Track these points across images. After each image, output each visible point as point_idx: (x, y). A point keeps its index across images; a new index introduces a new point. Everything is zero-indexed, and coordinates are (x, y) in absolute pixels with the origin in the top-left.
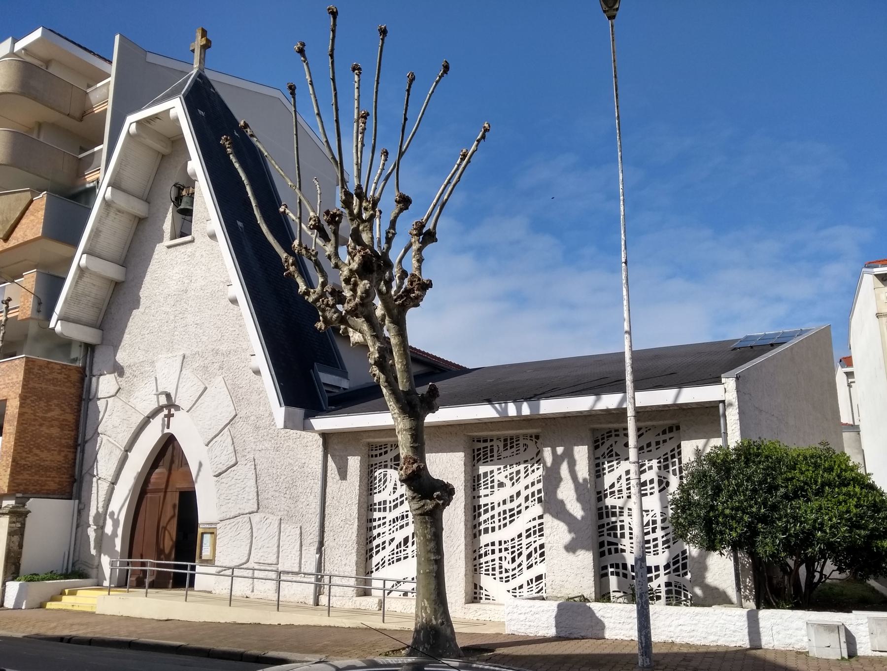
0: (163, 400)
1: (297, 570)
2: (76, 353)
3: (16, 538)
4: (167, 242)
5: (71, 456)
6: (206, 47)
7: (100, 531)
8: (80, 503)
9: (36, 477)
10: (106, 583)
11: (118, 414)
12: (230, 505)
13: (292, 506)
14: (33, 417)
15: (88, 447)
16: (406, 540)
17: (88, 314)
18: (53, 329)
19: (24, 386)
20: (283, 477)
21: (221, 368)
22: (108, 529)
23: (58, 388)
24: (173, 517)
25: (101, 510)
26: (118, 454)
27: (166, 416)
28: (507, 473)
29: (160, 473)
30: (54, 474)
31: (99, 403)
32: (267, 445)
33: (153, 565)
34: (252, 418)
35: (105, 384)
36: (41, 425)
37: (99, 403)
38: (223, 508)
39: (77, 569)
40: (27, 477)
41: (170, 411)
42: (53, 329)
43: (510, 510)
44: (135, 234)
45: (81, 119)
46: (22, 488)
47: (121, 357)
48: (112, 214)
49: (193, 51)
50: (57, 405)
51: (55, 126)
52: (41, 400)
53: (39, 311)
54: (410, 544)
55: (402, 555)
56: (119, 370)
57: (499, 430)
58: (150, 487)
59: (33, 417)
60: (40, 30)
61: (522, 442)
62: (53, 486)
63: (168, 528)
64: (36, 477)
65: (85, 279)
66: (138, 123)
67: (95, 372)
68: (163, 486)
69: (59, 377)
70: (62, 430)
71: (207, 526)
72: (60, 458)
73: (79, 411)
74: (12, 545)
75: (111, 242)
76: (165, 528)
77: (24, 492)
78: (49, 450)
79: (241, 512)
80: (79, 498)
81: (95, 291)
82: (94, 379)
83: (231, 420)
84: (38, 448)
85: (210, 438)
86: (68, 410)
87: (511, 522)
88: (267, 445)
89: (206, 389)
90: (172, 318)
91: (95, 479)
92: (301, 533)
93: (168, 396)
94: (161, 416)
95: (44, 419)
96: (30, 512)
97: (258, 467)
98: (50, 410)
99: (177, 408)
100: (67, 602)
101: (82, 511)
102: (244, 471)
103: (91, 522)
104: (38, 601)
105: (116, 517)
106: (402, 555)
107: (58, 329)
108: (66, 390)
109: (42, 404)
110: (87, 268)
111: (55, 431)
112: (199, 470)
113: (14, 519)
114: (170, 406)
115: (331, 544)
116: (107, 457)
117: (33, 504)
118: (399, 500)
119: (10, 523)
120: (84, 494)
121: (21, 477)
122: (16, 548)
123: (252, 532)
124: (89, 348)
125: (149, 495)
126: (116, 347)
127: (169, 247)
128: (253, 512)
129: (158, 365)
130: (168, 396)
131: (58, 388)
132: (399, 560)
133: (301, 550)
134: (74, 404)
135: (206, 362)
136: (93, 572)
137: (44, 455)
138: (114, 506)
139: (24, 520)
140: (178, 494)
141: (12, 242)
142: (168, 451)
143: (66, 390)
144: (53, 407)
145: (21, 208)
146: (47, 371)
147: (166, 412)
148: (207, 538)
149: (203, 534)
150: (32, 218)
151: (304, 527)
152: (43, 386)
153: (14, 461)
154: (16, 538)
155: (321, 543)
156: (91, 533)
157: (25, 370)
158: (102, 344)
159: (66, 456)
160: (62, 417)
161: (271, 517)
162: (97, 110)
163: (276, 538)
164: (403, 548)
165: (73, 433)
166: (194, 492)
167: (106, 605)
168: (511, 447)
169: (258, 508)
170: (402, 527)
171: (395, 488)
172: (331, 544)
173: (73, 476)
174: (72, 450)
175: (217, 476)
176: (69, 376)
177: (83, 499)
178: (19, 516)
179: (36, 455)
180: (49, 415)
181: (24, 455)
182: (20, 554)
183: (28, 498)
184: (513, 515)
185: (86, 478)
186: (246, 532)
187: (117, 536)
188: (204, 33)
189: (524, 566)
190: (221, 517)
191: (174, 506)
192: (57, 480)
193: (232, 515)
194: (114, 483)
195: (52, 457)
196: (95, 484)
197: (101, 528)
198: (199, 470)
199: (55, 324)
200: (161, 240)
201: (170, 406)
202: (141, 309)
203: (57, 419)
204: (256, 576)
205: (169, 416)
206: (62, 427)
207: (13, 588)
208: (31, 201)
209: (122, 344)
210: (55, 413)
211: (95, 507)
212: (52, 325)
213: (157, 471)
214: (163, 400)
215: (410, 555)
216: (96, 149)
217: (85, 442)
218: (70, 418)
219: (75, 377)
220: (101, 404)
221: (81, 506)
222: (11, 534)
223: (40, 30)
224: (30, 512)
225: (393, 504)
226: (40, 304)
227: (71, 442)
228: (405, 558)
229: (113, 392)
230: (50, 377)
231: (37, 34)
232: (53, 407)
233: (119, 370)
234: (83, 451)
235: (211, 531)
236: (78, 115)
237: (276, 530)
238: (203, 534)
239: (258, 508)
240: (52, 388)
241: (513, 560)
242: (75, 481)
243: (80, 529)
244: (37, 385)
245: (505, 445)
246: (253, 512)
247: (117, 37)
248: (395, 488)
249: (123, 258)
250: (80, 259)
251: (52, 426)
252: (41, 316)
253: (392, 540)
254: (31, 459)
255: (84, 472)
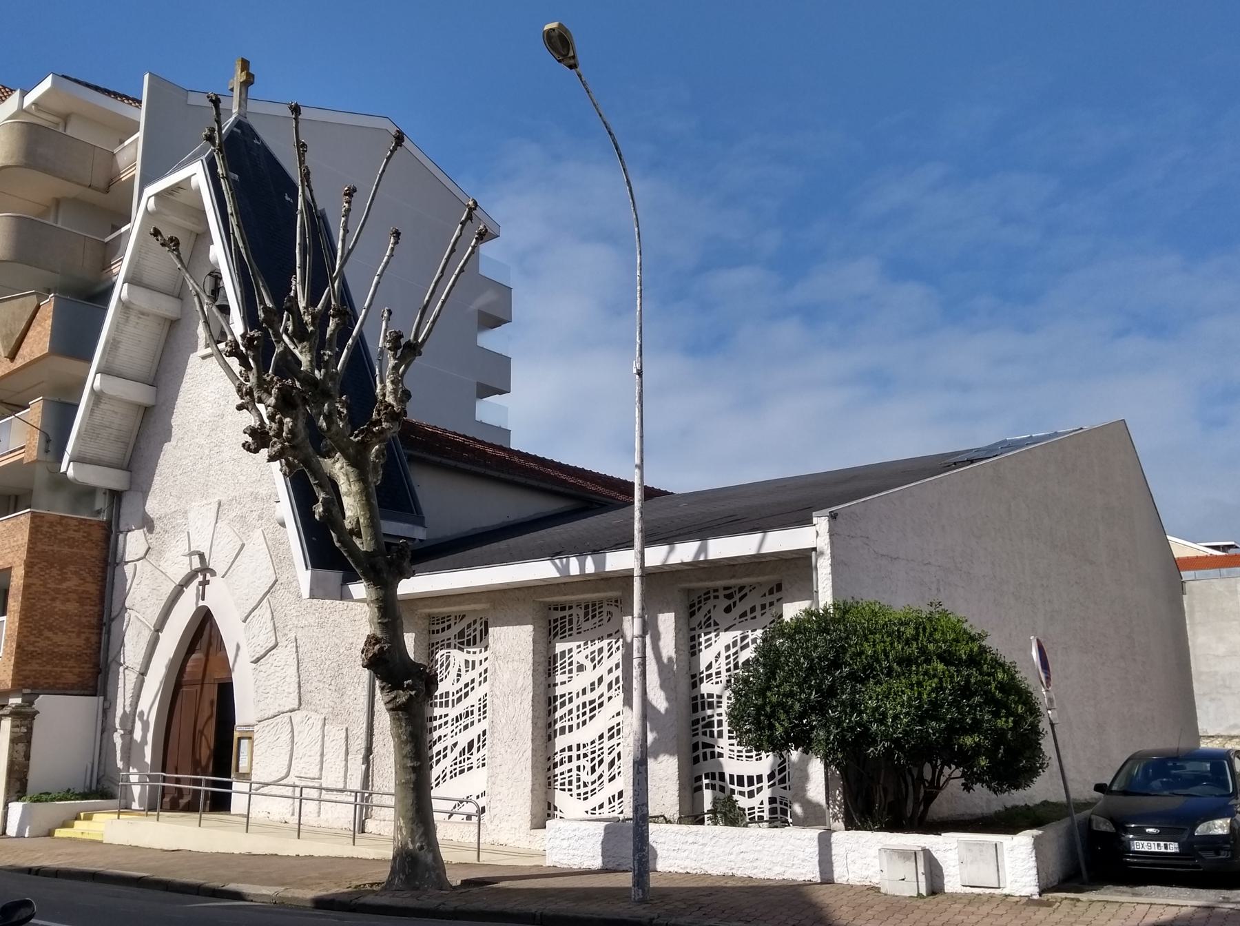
0: (196, 563)
1: (341, 786)
2: (101, 503)
3: (21, 747)
4: (202, 351)
5: (94, 639)
6: (248, 82)
7: (128, 737)
8: (105, 700)
9: (49, 668)
10: (135, 806)
11: (147, 582)
12: (268, 701)
13: (338, 701)
14: (42, 589)
15: (114, 625)
16: (471, 745)
17: (111, 451)
18: (65, 473)
19: (30, 550)
20: (328, 662)
21: (260, 518)
22: (137, 735)
23: (75, 550)
24: (211, 716)
25: (128, 709)
26: (147, 635)
27: (200, 584)
28: (588, 652)
29: (197, 660)
30: (72, 663)
31: (126, 567)
33: (209, 783)
35: (134, 543)
36: (53, 599)
37: (126, 567)
38: (261, 706)
39: (101, 788)
40: (36, 667)
42: (65, 473)
43: (592, 702)
44: (166, 341)
45: (107, 190)
46: (30, 681)
47: (152, 506)
48: (133, 319)
49: (232, 90)
50: (75, 573)
51: (77, 202)
52: (52, 566)
53: (47, 451)
54: (474, 750)
55: (466, 765)
56: (148, 524)
57: (573, 594)
58: (186, 678)
59: (42, 589)
60: (50, 78)
61: (605, 609)
62: (71, 678)
63: (205, 732)
64: (49, 668)
65: (102, 406)
66: (157, 195)
67: (122, 527)
68: (200, 677)
69: (77, 535)
70: (82, 605)
72: (80, 642)
73: (104, 579)
74: (16, 755)
75: (136, 353)
76: (202, 732)
77: (34, 686)
78: (64, 632)
79: (282, 709)
80: (105, 695)
81: (118, 421)
82: (121, 537)
83: (271, 587)
84: (50, 629)
85: (247, 611)
86: (90, 579)
87: (591, 718)
89: (243, 545)
90: (207, 452)
91: (121, 669)
92: (347, 737)
93: (202, 556)
94: (196, 583)
95: (57, 591)
96: (37, 712)
97: (300, 650)
98: (65, 579)
99: (213, 573)
100: (81, 829)
101: (107, 711)
102: (285, 654)
103: (117, 726)
104: (45, 826)
106: (466, 765)
107: (70, 473)
108: (85, 552)
109: (55, 572)
110: (101, 391)
111: (72, 607)
112: (237, 655)
113: (18, 723)
114: (202, 572)
115: (381, 751)
116: (135, 639)
117: (43, 703)
118: (464, 691)
119: (13, 727)
120: (110, 688)
121: (28, 668)
122: (21, 759)
123: (293, 736)
124: (116, 496)
125: (184, 689)
126: (145, 494)
127: (204, 358)
128: (293, 710)
129: (191, 515)
130: (202, 556)
131: (75, 550)
132: (462, 772)
133: (346, 760)
134: (97, 570)
135: (244, 510)
136: (118, 792)
137: (59, 638)
138: (143, 705)
139: (31, 724)
141: (19, 362)
142: (203, 630)
143: (85, 552)
144: (69, 575)
145: (27, 317)
146: (59, 529)
147: (200, 578)
148: (245, 743)
149: (239, 739)
150: (39, 329)
151: (350, 729)
152: (56, 548)
153: (18, 646)
154: (21, 747)
155: (369, 750)
156: (118, 739)
157: (31, 528)
158: (130, 489)
159: (87, 639)
160: (81, 589)
161: (314, 715)
162: (124, 177)
163: (319, 743)
164: (467, 755)
165: (96, 609)
166: (231, 684)
167: (133, 833)
168: (594, 616)
169: (300, 704)
170: (466, 727)
171: (459, 675)
172: (381, 751)
173: (97, 665)
174: (96, 631)
175: (256, 661)
176: (89, 534)
177: (109, 696)
178: (24, 718)
179: (48, 638)
180: (64, 586)
181: (32, 639)
182: (27, 767)
183: (38, 695)
184: (594, 709)
185: (113, 666)
186: (286, 737)
188: (245, 65)
189: (606, 778)
190: (259, 716)
191: (212, 703)
192: (77, 670)
193: (271, 713)
194: (143, 674)
195: (70, 641)
196: (121, 676)
197: (129, 732)
198: (237, 655)
199: (68, 468)
200: (195, 349)
201: (202, 572)
202: (173, 442)
203: (75, 591)
204: (323, 797)
205: (205, 583)
206: (81, 601)
207: (16, 808)
208: (38, 307)
210: (72, 583)
211: (122, 704)
212: (63, 469)
213: (194, 656)
214: (196, 563)
215: (475, 766)
216: (123, 229)
217: (111, 620)
218: (92, 588)
219: (97, 534)
220: (128, 569)
221: (107, 705)
222: (14, 741)
223: (50, 78)
224: (37, 712)
225: (456, 696)
226: (48, 441)
227: (94, 621)
228: (470, 769)
229: (141, 554)
230: (64, 536)
231: (47, 84)
232: (69, 575)
233: (148, 524)
234: (109, 632)
235: (248, 735)
236: (102, 184)
237: (319, 733)
238: (239, 739)
239: (300, 704)
240: (66, 550)
241: (593, 770)
242: (99, 673)
243: (105, 735)
244: (47, 548)
245: (586, 614)
246: (293, 710)
247: (147, 77)
248: (459, 675)
249: (153, 374)
250: (94, 380)
251: (68, 600)
252: (50, 458)
253: (455, 745)
254: (42, 643)
255: (110, 659)
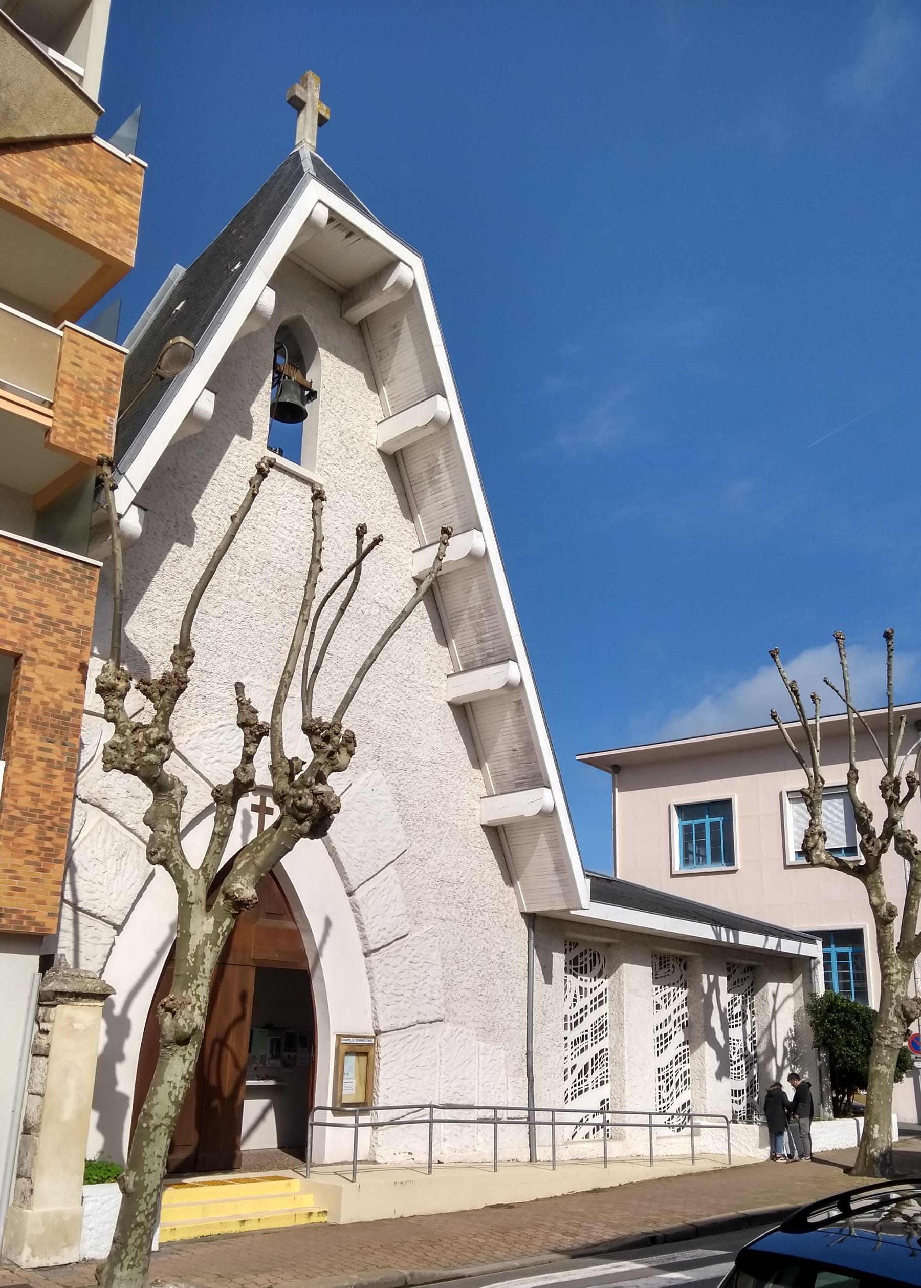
16: (586, 1066)
24: (241, 1018)
27: (255, 808)
28: (662, 994)
32: (455, 913)
34: (430, 862)
41: (263, 800)
43: (666, 1035)
54: (589, 1072)
55: (583, 1086)
61: (671, 962)
63: (231, 1041)
71: (355, 1040)
79: (421, 1018)
87: (666, 1047)
88: (455, 913)
105: (117, 1011)
106: (583, 1086)
112: (326, 934)
118: (580, 1016)
132: (580, 1093)
140: (252, 973)
164: (584, 1077)
168: (665, 967)
170: (582, 1050)
171: (575, 1000)
184: (666, 1041)
187: (121, 1058)
189: (674, 1095)
191: (243, 997)
193: (407, 1022)
198: (326, 934)
209: (143, 605)
215: (590, 1087)
225: (574, 1020)
228: (586, 1090)
235: (358, 1050)
241: (668, 1089)
245: (660, 964)
248: (575, 1000)
253: (574, 1067)
